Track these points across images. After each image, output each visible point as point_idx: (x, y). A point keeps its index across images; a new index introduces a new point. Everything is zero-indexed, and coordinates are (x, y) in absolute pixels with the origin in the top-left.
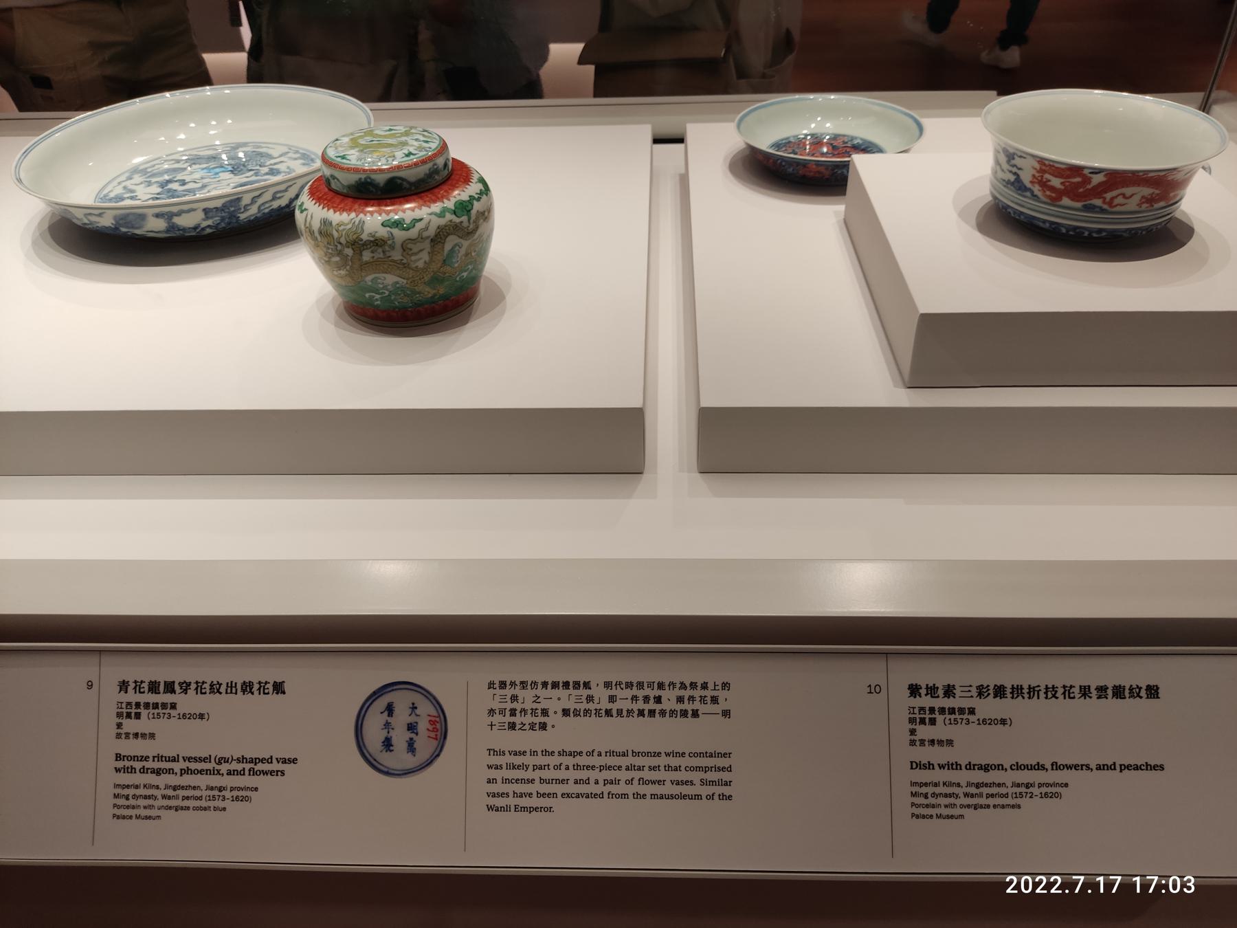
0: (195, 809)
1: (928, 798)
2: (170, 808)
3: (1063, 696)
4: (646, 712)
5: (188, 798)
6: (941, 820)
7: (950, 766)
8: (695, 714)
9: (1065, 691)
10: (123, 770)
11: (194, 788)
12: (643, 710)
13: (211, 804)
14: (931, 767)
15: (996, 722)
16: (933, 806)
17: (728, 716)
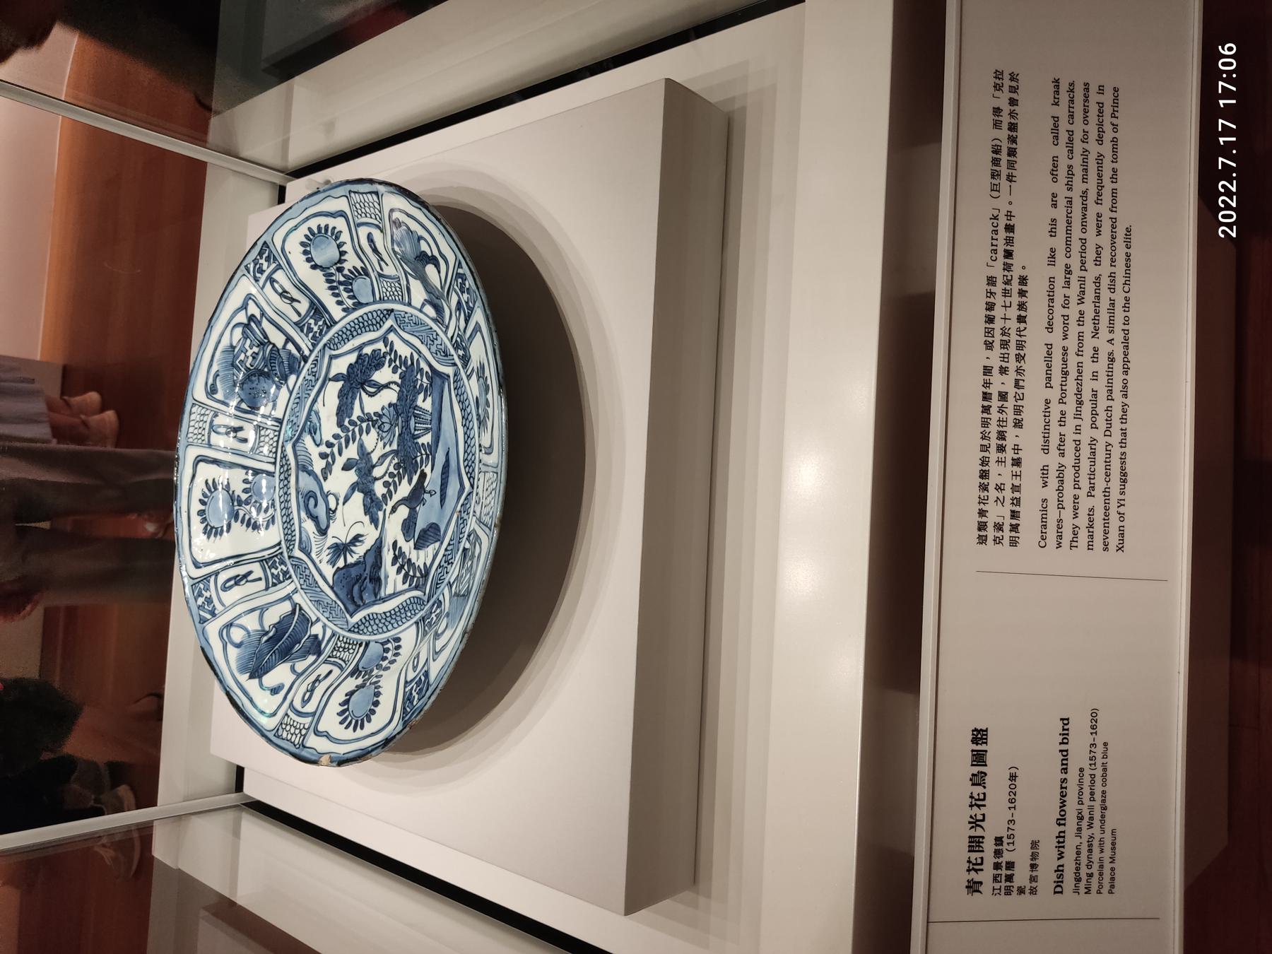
0: (1104, 783)
1: (1092, 873)
2: (1103, 816)
3: (981, 808)
4: (1014, 522)
5: (1092, 794)
6: (1117, 857)
7: (1061, 845)
8: (1023, 280)
9: (973, 869)
10: (1060, 849)
11: (1078, 853)
12: (1011, 525)
13: (1099, 761)
14: (1061, 868)
15: (1013, 787)
16: (1101, 866)
17: (1021, 408)
